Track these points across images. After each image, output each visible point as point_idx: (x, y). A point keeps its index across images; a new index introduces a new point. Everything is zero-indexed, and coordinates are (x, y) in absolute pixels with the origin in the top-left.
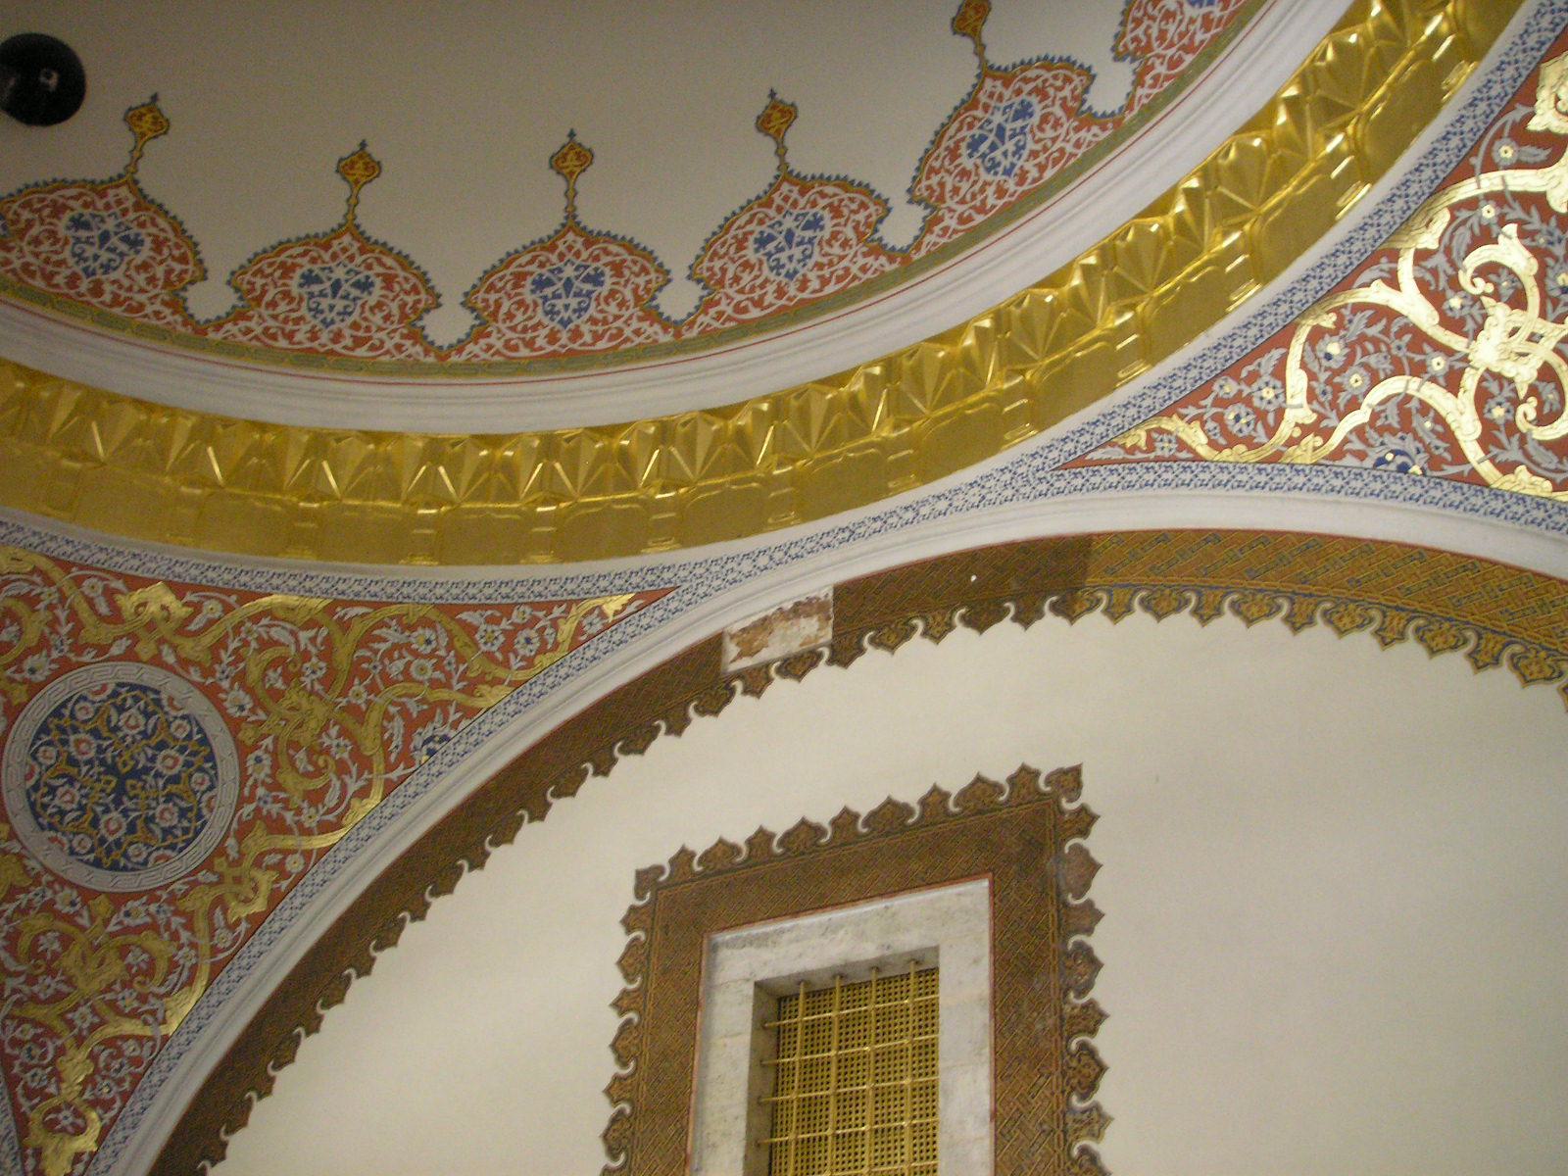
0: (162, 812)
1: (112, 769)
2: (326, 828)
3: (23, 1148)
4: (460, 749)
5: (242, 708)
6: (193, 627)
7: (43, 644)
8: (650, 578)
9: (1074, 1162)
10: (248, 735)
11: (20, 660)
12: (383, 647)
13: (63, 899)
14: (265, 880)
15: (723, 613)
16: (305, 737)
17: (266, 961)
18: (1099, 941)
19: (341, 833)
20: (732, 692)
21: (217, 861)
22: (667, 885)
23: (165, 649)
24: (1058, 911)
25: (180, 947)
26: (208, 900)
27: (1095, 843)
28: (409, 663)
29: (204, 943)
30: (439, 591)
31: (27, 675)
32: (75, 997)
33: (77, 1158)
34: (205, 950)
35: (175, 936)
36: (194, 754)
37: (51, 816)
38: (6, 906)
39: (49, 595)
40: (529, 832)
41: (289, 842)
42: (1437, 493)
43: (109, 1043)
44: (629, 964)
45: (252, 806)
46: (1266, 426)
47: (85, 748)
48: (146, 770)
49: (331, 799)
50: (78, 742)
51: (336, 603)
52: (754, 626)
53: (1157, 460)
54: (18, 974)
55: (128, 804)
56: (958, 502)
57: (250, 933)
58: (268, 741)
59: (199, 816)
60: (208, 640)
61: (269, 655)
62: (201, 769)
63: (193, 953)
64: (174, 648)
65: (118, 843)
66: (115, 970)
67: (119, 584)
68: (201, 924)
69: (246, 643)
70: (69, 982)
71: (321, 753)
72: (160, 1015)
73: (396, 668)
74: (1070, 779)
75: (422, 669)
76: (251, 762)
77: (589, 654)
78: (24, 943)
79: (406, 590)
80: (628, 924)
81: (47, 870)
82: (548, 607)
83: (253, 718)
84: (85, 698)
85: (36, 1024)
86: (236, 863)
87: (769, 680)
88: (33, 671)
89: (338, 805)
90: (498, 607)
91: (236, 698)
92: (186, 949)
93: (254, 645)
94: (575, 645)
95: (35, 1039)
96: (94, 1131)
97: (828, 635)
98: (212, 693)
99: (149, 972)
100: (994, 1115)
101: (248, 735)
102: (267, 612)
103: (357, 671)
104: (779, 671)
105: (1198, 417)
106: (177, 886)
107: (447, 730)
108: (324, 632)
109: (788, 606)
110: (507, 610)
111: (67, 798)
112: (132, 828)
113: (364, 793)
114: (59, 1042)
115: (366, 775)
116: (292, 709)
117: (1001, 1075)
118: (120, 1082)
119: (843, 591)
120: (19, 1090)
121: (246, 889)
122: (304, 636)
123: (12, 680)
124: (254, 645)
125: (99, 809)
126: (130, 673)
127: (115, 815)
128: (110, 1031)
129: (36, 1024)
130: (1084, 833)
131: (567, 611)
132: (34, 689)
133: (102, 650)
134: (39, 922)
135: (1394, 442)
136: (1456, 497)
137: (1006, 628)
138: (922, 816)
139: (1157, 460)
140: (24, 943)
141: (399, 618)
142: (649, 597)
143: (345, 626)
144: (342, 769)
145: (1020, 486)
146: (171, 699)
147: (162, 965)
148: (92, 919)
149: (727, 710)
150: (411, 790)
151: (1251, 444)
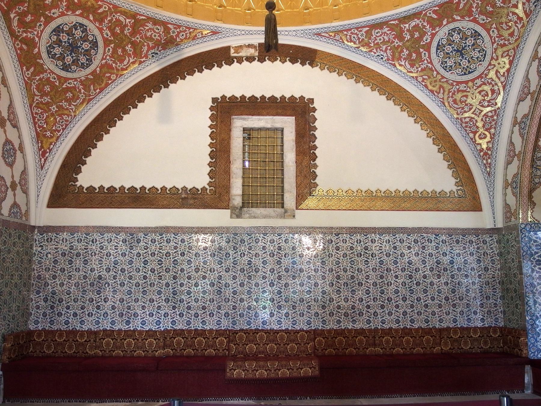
4: (160, 57)
5: (107, 35)
8: (215, 28)
12: (147, 28)
15: (232, 42)
19: (127, 71)
20: (234, 61)
22: (220, 102)
23: (91, 16)
25: (81, 93)
28: (152, 34)
30: (164, 18)
31: (52, 15)
42: (387, 65)
44: (212, 118)
46: (359, 41)
47: (64, 37)
48: (80, 47)
49: (125, 63)
50: (63, 36)
52: (238, 47)
53: (335, 40)
55: (73, 55)
56: (290, 33)
57: (100, 93)
58: (112, 45)
59: (91, 61)
69: (112, 19)
70: (51, 99)
73: (149, 34)
74: (312, 101)
75: (155, 36)
76: (107, 50)
77: (197, 42)
79: (156, 15)
82: (189, 28)
84: (67, 24)
85: (41, 109)
87: (243, 61)
88: (53, 14)
93: (114, 20)
94: (194, 39)
95: (42, 112)
97: (257, 54)
98: (101, 30)
100: (296, 162)
104: (245, 59)
105: (347, 35)
106: (82, 78)
107: (158, 52)
108: (133, 21)
109: (247, 44)
110: (179, 27)
113: (134, 63)
117: (297, 155)
118: (62, 126)
122: (128, 20)
126: (81, 20)
127: (70, 57)
128: (60, 112)
130: (314, 112)
131: (194, 31)
132: (52, 19)
136: (390, 67)
139: (335, 40)
142: (214, 33)
145: (305, 34)
146: (90, 29)
149: (232, 65)
150: (146, 65)
151: (355, 43)
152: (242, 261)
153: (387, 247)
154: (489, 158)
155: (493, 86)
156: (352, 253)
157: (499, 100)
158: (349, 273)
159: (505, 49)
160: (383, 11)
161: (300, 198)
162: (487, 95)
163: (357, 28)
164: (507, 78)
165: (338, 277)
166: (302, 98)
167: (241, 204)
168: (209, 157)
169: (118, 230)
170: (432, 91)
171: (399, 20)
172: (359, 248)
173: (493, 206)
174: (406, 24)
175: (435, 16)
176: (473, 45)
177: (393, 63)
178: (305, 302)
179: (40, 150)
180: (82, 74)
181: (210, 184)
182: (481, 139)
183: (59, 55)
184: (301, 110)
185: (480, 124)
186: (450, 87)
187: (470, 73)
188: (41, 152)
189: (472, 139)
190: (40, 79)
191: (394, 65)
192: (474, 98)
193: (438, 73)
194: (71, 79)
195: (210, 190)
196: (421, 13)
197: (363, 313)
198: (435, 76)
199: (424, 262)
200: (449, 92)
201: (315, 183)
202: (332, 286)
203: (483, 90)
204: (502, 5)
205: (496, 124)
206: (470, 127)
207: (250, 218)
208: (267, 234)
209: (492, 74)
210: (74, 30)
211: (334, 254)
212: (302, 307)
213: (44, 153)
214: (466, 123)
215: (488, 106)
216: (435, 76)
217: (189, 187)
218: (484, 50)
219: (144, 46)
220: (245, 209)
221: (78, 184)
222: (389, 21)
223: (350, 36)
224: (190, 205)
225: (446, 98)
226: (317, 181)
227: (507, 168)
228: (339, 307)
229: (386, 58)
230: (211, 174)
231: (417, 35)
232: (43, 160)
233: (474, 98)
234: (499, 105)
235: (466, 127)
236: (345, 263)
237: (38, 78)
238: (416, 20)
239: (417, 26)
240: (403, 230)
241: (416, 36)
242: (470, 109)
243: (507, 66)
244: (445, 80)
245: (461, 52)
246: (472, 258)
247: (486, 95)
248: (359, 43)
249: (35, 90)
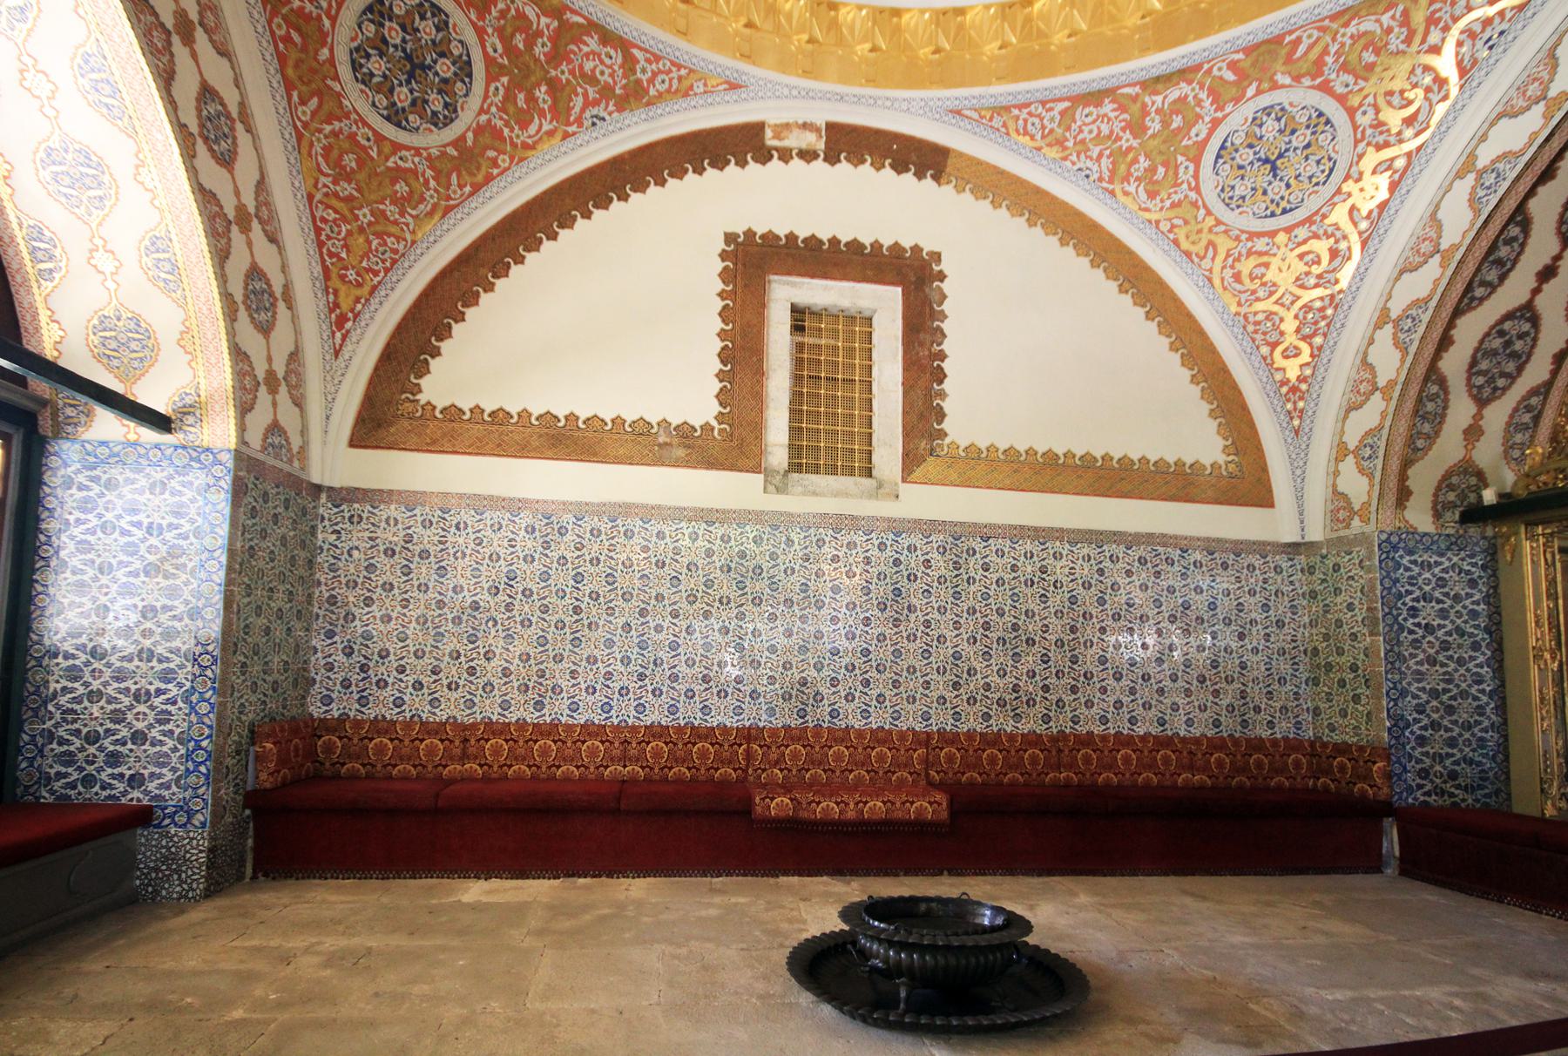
18: (946, 326)
44: (725, 275)
65: (403, 109)
70: (359, 190)
74: (937, 257)
85: (336, 212)
90: (654, 55)
95: (335, 220)
105: (1017, 118)
111: (377, 65)
117: (907, 368)
118: (383, 261)
119: (832, 128)
124: (513, 12)
127: (405, 90)
128: (379, 228)
135: (1089, 164)
137: (909, 177)
140: (335, 153)
148: (379, 153)
151: (1032, 138)
153: (1085, 571)
154: (1301, 398)
155: (1337, 242)
157: (1346, 275)
159: (1387, 153)
160: (1110, 63)
161: (911, 461)
162: (1318, 262)
163: (1043, 103)
164: (1374, 224)
166: (916, 249)
167: (785, 465)
168: (717, 360)
169: (514, 506)
170: (1188, 254)
171: (1144, 84)
172: (1029, 569)
173: (1300, 498)
174: (1156, 93)
175: (1230, 76)
176: (1308, 146)
177: (1111, 187)
179: (331, 311)
180: (434, 140)
181: (720, 417)
182: (1287, 357)
184: (914, 274)
185: (1289, 326)
186: (1233, 244)
187: (1285, 211)
189: (1265, 359)
190: (335, 134)
191: (1112, 193)
192: (1284, 268)
193: (1209, 213)
194: (408, 148)
195: (720, 431)
196: (1197, 68)
198: (1200, 218)
199: (1158, 603)
200: (1228, 256)
203: (1308, 253)
204: (1402, 47)
205: (1328, 325)
206: (1265, 334)
207: (804, 494)
209: (1339, 215)
213: (341, 321)
214: (1257, 323)
215: (1317, 286)
216: (1200, 218)
218: (1330, 159)
220: (796, 475)
221: (423, 398)
222: (1119, 87)
223: (1025, 121)
224: (677, 460)
225: (1217, 269)
226: (946, 425)
227: (1345, 418)
229: (1096, 176)
231: (1177, 122)
232: (338, 335)
233: (1284, 268)
234: (1343, 284)
235: (1256, 332)
236: (1001, 598)
237: (328, 128)
238: (1183, 85)
239: (1183, 100)
240: (1117, 537)
241: (1174, 125)
242: (1271, 294)
243: (1383, 194)
244: (1222, 228)
245: (1273, 164)
246: (1252, 600)
247: (1314, 263)
248: (1043, 137)
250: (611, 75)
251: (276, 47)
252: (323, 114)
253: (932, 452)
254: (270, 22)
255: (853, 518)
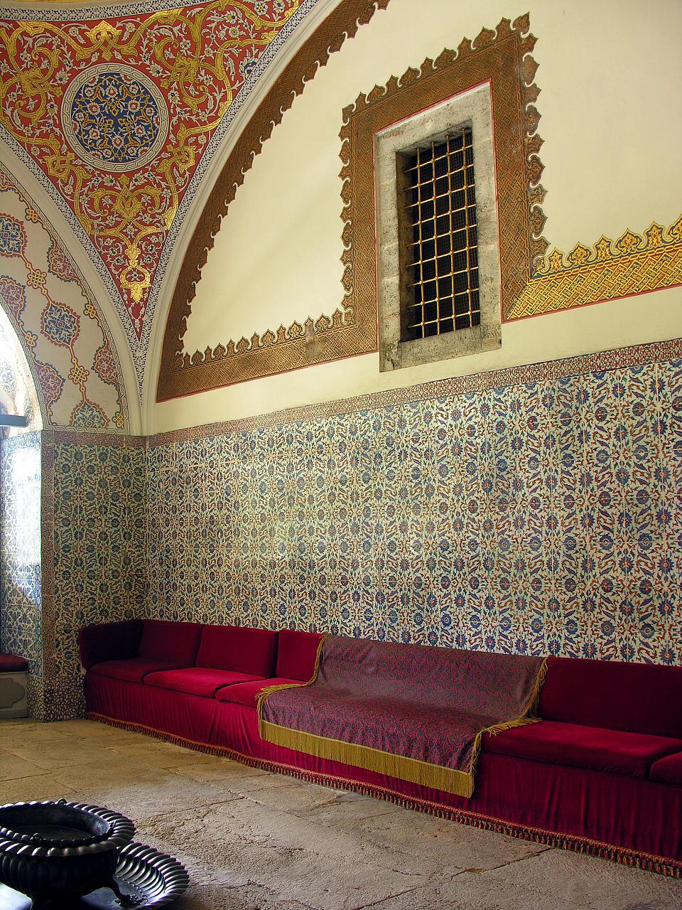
0: (137, 131)
1: (110, 116)
2: (211, 119)
3: (121, 290)
5: (158, 72)
6: (124, 39)
7: (61, 65)
9: (532, 214)
10: (165, 84)
11: (53, 76)
12: (213, 25)
13: (107, 180)
14: (191, 150)
16: (191, 79)
17: (201, 187)
18: (539, 105)
20: (374, 7)
21: (168, 147)
23: (115, 52)
24: (521, 92)
26: (169, 165)
27: (536, 54)
29: (172, 185)
31: (59, 82)
32: (125, 222)
33: (144, 290)
34: (174, 189)
35: (159, 185)
36: (143, 100)
37: (90, 144)
38: (84, 189)
39: (56, 41)
40: (297, 100)
41: (197, 130)
43: (145, 239)
44: (343, 156)
45: (177, 116)
48: (125, 112)
49: (210, 105)
51: (186, 9)
54: (98, 218)
57: (191, 176)
59: (154, 128)
60: (133, 43)
61: (162, 43)
62: (149, 106)
63: (169, 191)
64: (119, 51)
65: (122, 149)
66: (138, 206)
67: (85, 27)
68: (169, 177)
69: (151, 40)
70: (120, 216)
71: (200, 85)
72: (162, 222)
73: (222, 34)
74: (524, 21)
76: (170, 97)
78: (96, 203)
80: (342, 136)
81: (96, 169)
83: (165, 75)
85: (112, 238)
86: (176, 146)
89: (214, 108)
91: (154, 68)
92: (166, 190)
93: (154, 40)
96: (148, 279)
98: (143, 68)
99: (153, 204)
101: (165, 84)
102: (155, 23)
103: (205, 41)
112: (126, 141)
113: (224, 99)
114: (124, 243)
115: (223, 90)
116: (181, 66)
120: (112, 267)
121: (184, 157)
122: (176, 29)
123: (53, 86)
125: (109, 136)
126: (103, 68)
127: (117, 136)
128: (143, 234)
129: (112, 238)
130: (531, 49)
132: (64, 87)
133: (88, 61)
134: (100, 193)
138: (460, 55)
140: (96, 203)
141: (216, 9)
143: (193, 19)
144: (211, 90)
146: (125, 76)
147: (157, 200)
148: (122, 186)
152: (403, 471)
156: (639, 424)
158: (633, 486)
161: (511, 290)
165: (605, 499)
167: (398, 336)
172: (659, 406)
178: (528, 570)
179: (128, 306)
183: (100, 141)
188: (130, 309)
194: (137, 172)
197: (671, 605)
201: (542, 240)
202: (590, 525)
208: (446, 397)
210: (102, 89)
211: (591, 432)
212: (522, 584)
213: (136, 310)
217: (315, 318)
219: (225, 60)
220: (408, 344)
221: (184, 351)
226: (547, 233)
228: (607, 586)
230: (347, 281)
232: (137, 321)
237: (86, 189)
249: (88, 210)
250: (241, 29)
251: (38, 163)
252: (79, 183)
253: (532, 273)
254: (29, 152)
255: (456, 380)
